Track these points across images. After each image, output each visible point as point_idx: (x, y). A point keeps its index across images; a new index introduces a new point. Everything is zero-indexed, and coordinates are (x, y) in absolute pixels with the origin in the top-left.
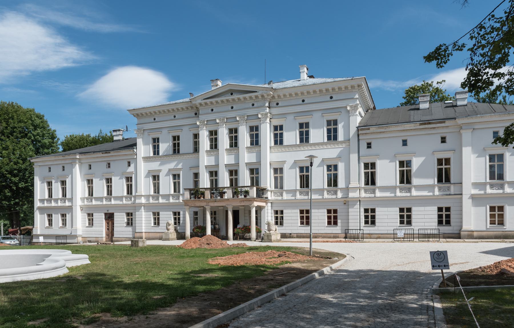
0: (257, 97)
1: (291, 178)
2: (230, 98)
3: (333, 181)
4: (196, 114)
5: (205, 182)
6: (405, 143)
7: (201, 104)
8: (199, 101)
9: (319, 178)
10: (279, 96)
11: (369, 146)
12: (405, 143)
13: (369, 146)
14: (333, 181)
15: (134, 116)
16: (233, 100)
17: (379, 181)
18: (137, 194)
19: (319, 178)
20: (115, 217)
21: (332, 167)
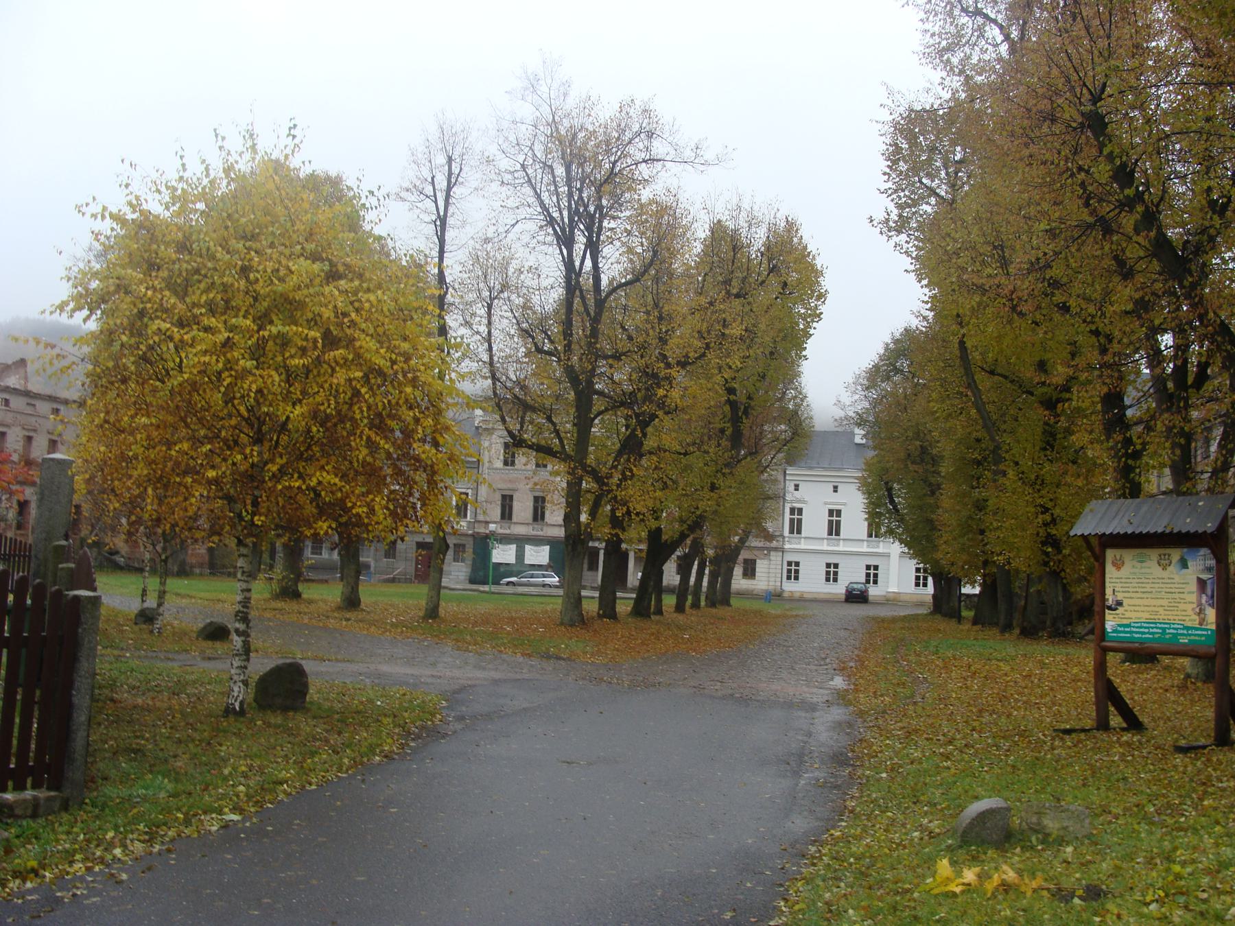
6: (835, 489)
11: (797, 487)
12: (835, 489)
13: (797, 487)
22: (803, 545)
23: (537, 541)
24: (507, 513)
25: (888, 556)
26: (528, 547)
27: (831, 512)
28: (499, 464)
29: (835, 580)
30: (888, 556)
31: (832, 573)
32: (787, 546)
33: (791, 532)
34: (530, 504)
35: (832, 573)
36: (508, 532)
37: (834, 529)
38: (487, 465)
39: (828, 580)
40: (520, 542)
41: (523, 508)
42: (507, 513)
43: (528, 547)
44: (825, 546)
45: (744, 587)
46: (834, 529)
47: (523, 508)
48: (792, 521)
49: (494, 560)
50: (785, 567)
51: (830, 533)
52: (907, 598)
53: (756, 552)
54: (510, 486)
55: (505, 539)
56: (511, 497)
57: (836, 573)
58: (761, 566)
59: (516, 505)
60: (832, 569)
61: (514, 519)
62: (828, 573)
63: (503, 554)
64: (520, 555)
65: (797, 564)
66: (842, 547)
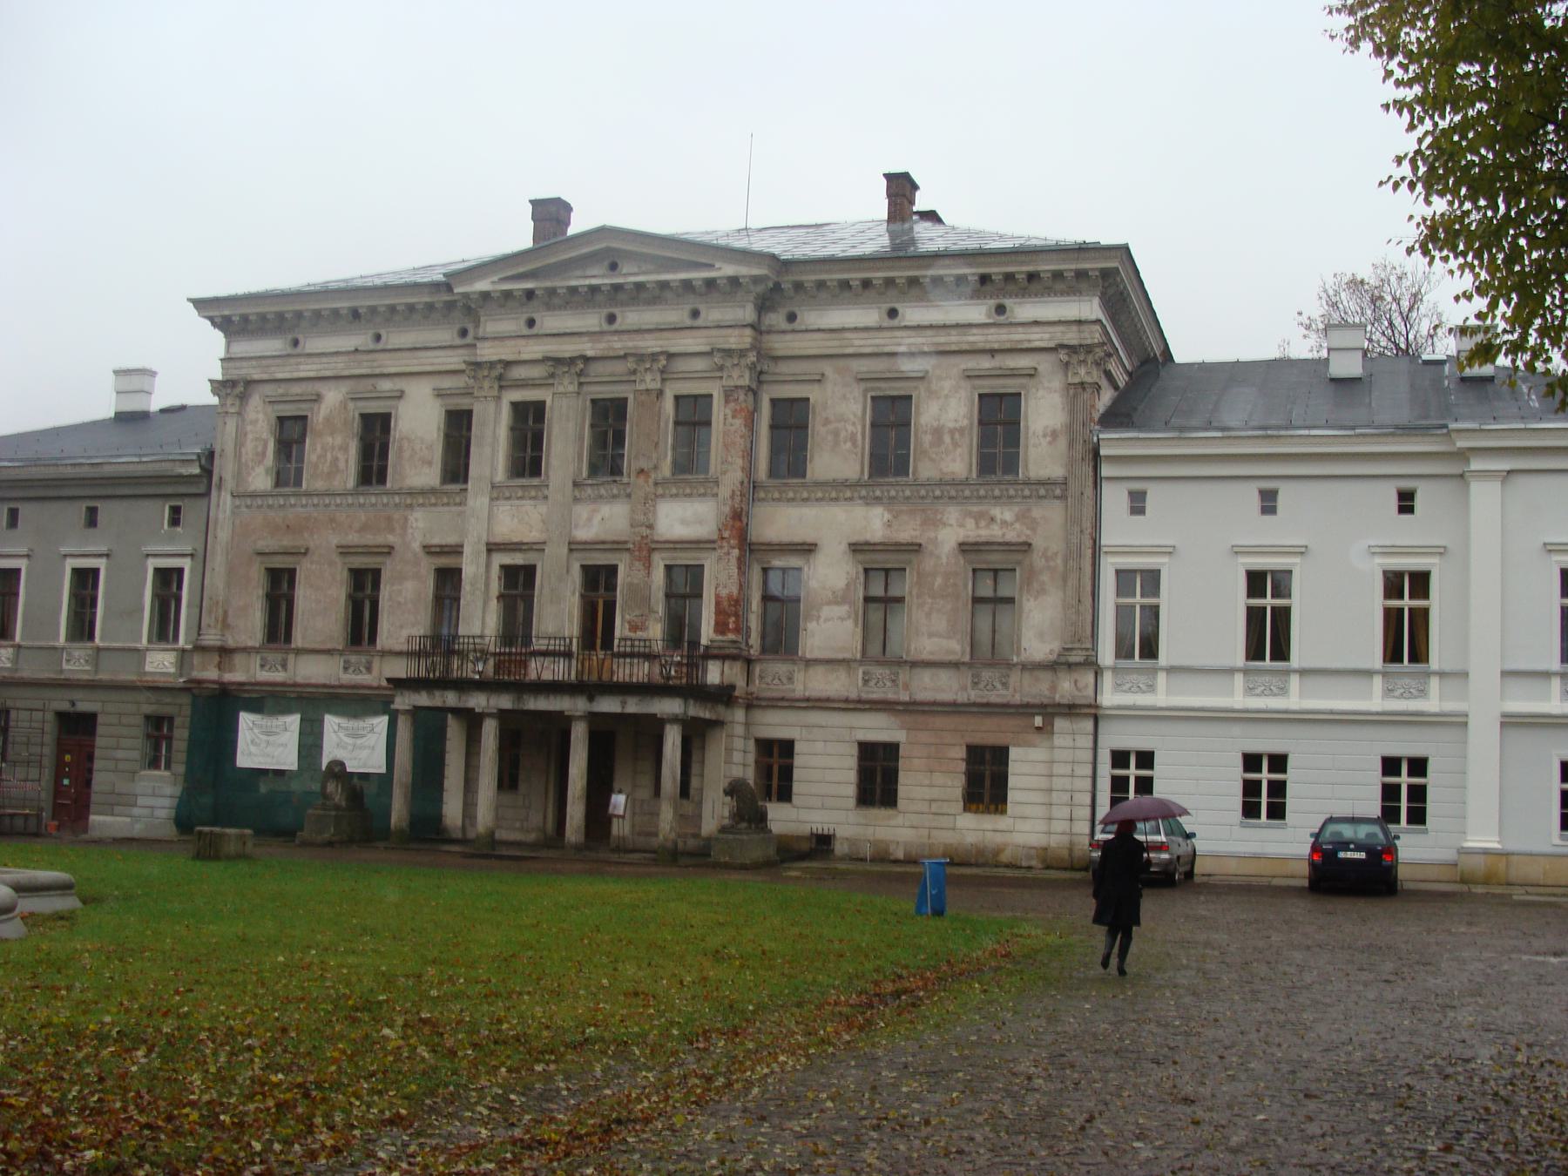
0: (710, 283)
4: (464, 333)
7: (486, 296)
10: (799, 286)
11: (1137, 504)
13: (1137, 504)
15: (214, 324)
16: (617, 288)
20: (100, 730)
22: (1164, 694)
23: (355, 702)
24: (279, 626)
25: (1459, 723)
26: (331, 722)
27: (1256, 581)
28: (261, 480)
29: (1277, 812)
30: (1459, 723)
31: (1264, 791)
32: (1109, 697)
33: (1123, 651)
34: (338, 593)
35: (1264, 791)
36: (279, 676)
37: (1268, 636)
38: (230, 483)
39: (1250, 810)
40: (313, 704)
41: (320, 607)
42: (279, 626)
43: (331, 722)
44: (1237, 696)
45: (971, 839)
46: (1268, 636)
47: (320, 607)
48: (1123, 613)
49: (243, 761)
50: (1106, 771)
51: (1254, 652)
52: (1534, 872)
53: (1011, 723)
54: (287, 542)
55: (268, 700)
56: (292, 573)
57: (1278, 789)
58: (1026, 767)
59: (304, 598)
60: (1265, 776)
61: (298, 640)
62: (1251, 789)
63: (265, 743)
64: (310, 743)
65: (1146, 759)
66: (1296, 698)
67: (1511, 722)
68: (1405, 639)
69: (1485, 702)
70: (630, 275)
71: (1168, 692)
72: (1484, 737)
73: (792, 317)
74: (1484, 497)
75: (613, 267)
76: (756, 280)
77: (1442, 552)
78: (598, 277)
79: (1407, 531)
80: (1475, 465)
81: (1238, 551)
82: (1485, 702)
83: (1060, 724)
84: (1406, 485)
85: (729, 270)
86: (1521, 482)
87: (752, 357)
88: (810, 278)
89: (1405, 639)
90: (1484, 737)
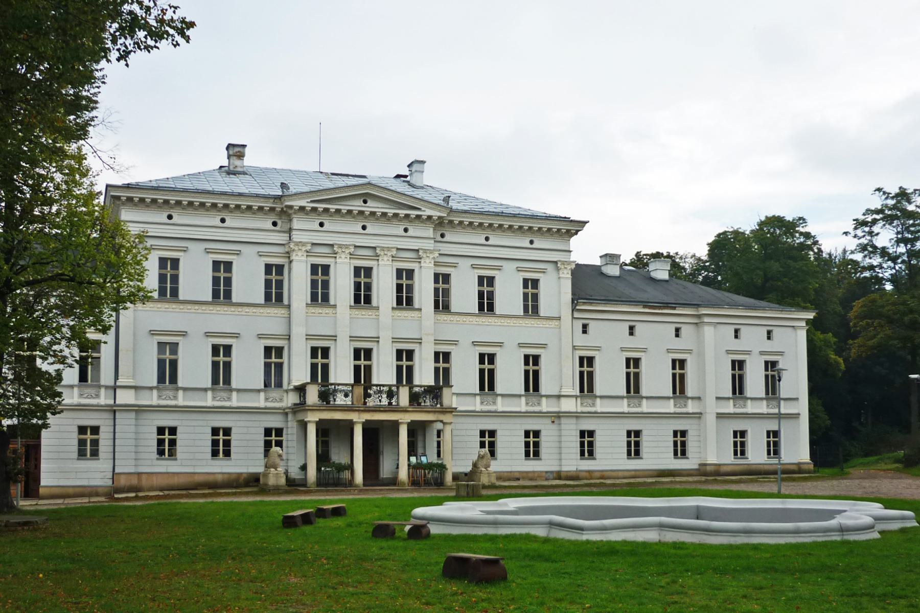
0: (418, 217)
1: (464, 374)
2: (357, 205)
3: (532, 382)
5: (298, 371)
6: (632, 330)
7: (302, 209)
8: (302, 203)
9: (509, 375)
10: (451, 222)
12: (632, 330)
14: (532, 382)
16: (373, 214)
17: (600, 388)
18: (118, 384)
19: (509, 375)
21: (532, 360)
30: (699, 416)
67: (720, 416)
68: (679, 385)
69: (712, 408)
70: (373, 206)
71: (601, 406)
72: (710, 419)
73: (442, 236)
74: (708, 331)
75: (365, 202)
76: (440, 218)
77: (689, 351)
78: (357, 205)
79: (677, 344)
80: (706, 320)
81: (669, 351)
82: (712, 408)
83: (563, 420)
84: (678, 326)
85: (429, 212)
86: (719, 326)
87: (436, 254)
88: (456, 220)
89: (679, 385)
90: (710, 419)
